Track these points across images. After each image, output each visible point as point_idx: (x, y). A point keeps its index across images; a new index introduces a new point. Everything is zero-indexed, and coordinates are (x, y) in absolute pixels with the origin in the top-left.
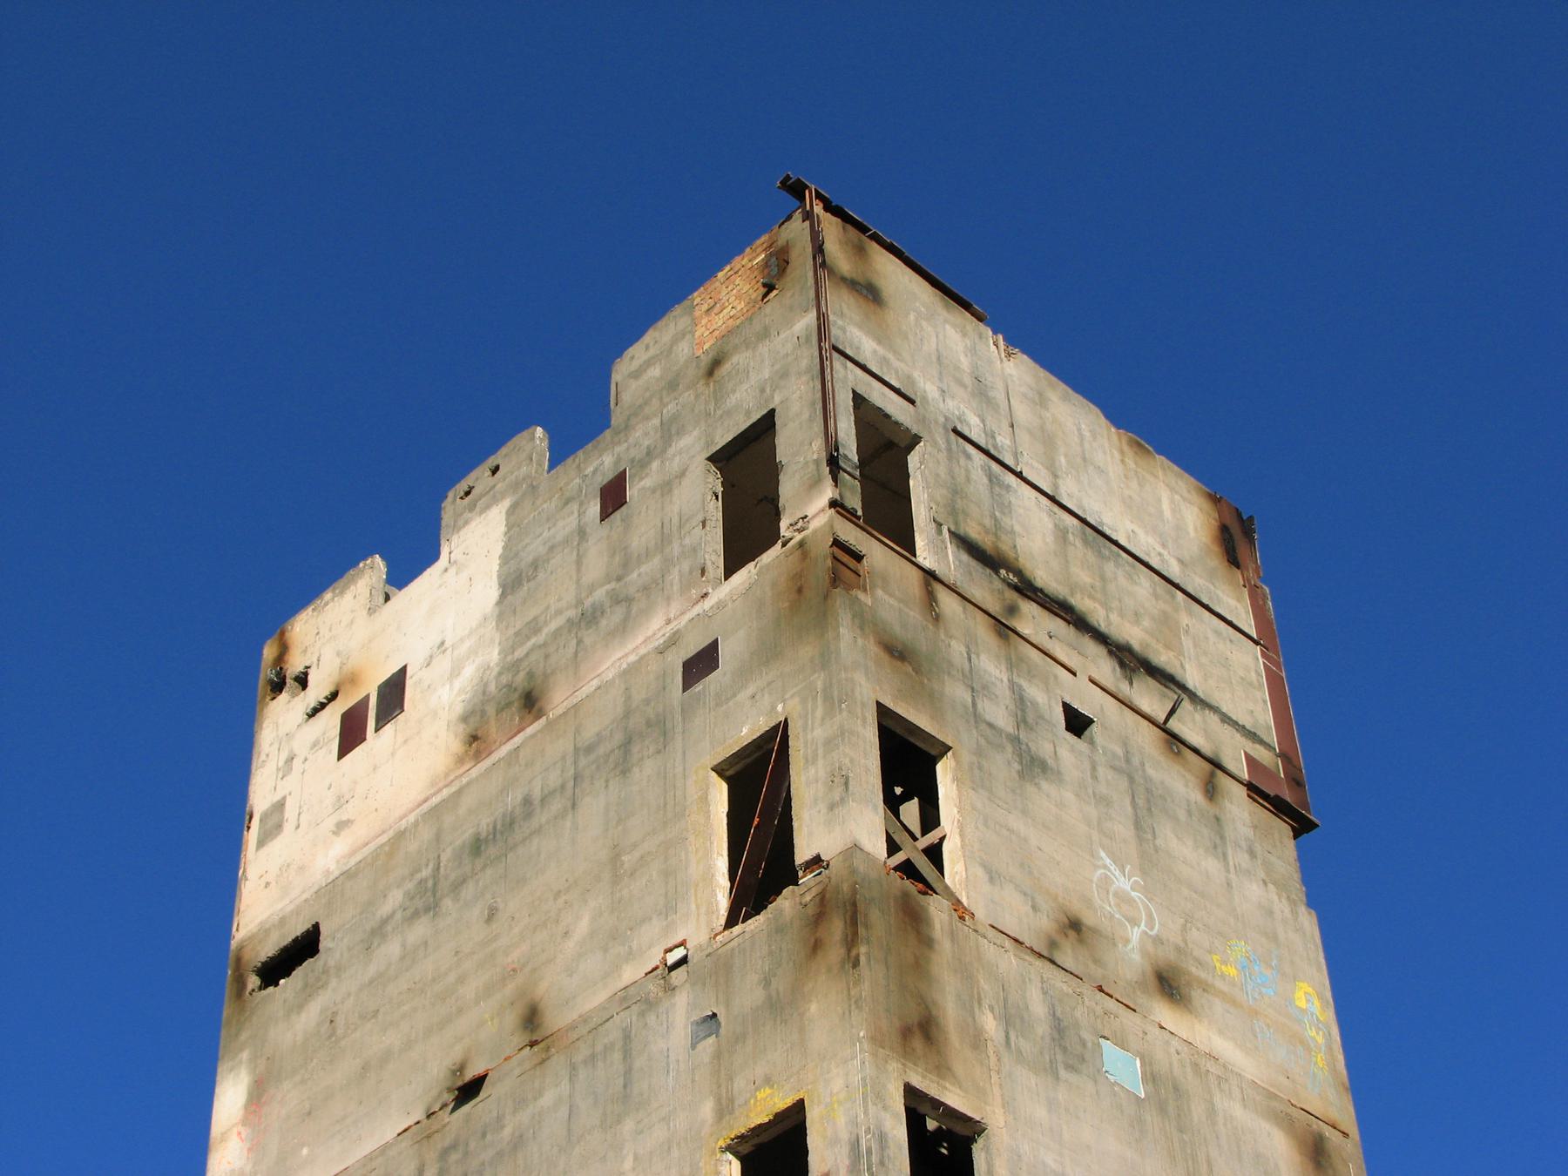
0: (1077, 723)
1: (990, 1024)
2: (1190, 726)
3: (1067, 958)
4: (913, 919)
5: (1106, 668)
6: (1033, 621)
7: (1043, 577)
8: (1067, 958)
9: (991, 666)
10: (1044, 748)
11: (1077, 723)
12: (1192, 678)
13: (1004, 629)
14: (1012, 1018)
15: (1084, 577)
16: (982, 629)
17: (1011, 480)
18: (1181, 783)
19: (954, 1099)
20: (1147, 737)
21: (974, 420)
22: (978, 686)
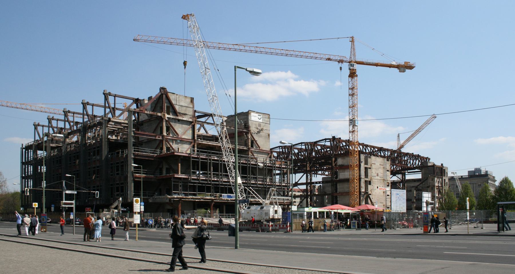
12: (187, 113)
15: (180, 110)
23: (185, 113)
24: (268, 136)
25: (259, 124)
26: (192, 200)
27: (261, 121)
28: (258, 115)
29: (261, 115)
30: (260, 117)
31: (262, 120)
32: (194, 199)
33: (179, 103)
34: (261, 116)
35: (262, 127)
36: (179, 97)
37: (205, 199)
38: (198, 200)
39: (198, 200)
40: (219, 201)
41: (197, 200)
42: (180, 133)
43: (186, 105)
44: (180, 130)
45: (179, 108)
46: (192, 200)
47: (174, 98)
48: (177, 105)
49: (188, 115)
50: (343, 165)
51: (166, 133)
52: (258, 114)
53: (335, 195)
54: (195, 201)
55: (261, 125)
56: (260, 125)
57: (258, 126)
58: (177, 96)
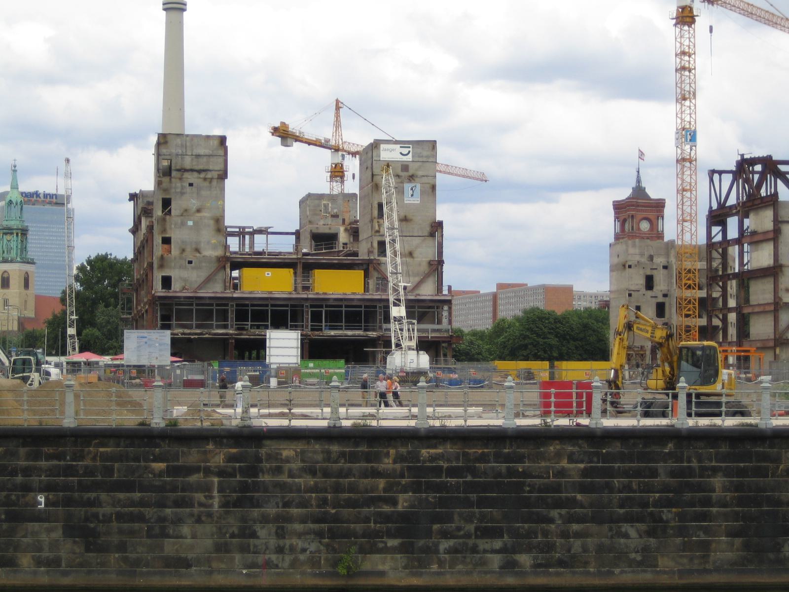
0: (191, 185)
1: (173, 226)
2: (209, 175)
3: (185, 214)
4: (164, 220)
5: (196, 174)
6: (186, 175)
7: (188, 167)
8: (185, 214)
9: (179, 185)
10: (185, 191)
11: (191, 185)
12: (211, 168)
13: (181, 179)
14: (175, 225)
15: (194, 163)
16: (178, 180)
17: (185, 156)
18: (206, 184)
19: (167, 236)
20: (200, 180)
21: (180, 151)
22: (175, 188)
23: (206, 168)
24: (431, 190)
25: (402, 165)
26: (183, 336)
27: (409, 158)
28: (401, 147)
29: (411, 146)
30: (405, 151)
31: (413, 156)
32: (189, 334)
33: (192, 151)
34: (410, 147)
35: (411, 172)
36: (192, 140)
37: (215, 334)
38: (196, 337)
39: (196, 337)
40: (248, 337)
41: (192, 337)
42: (195, 207)
43: (207, 152)
44: (194, 202)
45: (192, 159)
46: (183, 336)
47: (180, 143)
48: (186, 155)
49: (213, 172)
50: (756, 232)
51: (163, 212)
52: (399, 146)
53: (746, 311)
54: (190, 337)
55: (410, 168)
56: (405, 167)
57: (400, 170)
58: (188, 138)
